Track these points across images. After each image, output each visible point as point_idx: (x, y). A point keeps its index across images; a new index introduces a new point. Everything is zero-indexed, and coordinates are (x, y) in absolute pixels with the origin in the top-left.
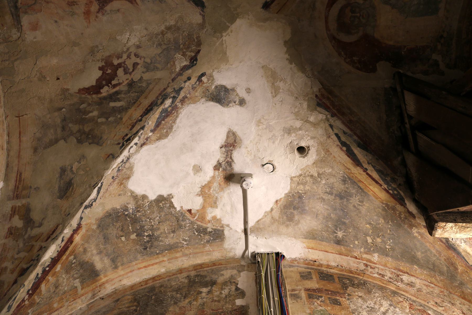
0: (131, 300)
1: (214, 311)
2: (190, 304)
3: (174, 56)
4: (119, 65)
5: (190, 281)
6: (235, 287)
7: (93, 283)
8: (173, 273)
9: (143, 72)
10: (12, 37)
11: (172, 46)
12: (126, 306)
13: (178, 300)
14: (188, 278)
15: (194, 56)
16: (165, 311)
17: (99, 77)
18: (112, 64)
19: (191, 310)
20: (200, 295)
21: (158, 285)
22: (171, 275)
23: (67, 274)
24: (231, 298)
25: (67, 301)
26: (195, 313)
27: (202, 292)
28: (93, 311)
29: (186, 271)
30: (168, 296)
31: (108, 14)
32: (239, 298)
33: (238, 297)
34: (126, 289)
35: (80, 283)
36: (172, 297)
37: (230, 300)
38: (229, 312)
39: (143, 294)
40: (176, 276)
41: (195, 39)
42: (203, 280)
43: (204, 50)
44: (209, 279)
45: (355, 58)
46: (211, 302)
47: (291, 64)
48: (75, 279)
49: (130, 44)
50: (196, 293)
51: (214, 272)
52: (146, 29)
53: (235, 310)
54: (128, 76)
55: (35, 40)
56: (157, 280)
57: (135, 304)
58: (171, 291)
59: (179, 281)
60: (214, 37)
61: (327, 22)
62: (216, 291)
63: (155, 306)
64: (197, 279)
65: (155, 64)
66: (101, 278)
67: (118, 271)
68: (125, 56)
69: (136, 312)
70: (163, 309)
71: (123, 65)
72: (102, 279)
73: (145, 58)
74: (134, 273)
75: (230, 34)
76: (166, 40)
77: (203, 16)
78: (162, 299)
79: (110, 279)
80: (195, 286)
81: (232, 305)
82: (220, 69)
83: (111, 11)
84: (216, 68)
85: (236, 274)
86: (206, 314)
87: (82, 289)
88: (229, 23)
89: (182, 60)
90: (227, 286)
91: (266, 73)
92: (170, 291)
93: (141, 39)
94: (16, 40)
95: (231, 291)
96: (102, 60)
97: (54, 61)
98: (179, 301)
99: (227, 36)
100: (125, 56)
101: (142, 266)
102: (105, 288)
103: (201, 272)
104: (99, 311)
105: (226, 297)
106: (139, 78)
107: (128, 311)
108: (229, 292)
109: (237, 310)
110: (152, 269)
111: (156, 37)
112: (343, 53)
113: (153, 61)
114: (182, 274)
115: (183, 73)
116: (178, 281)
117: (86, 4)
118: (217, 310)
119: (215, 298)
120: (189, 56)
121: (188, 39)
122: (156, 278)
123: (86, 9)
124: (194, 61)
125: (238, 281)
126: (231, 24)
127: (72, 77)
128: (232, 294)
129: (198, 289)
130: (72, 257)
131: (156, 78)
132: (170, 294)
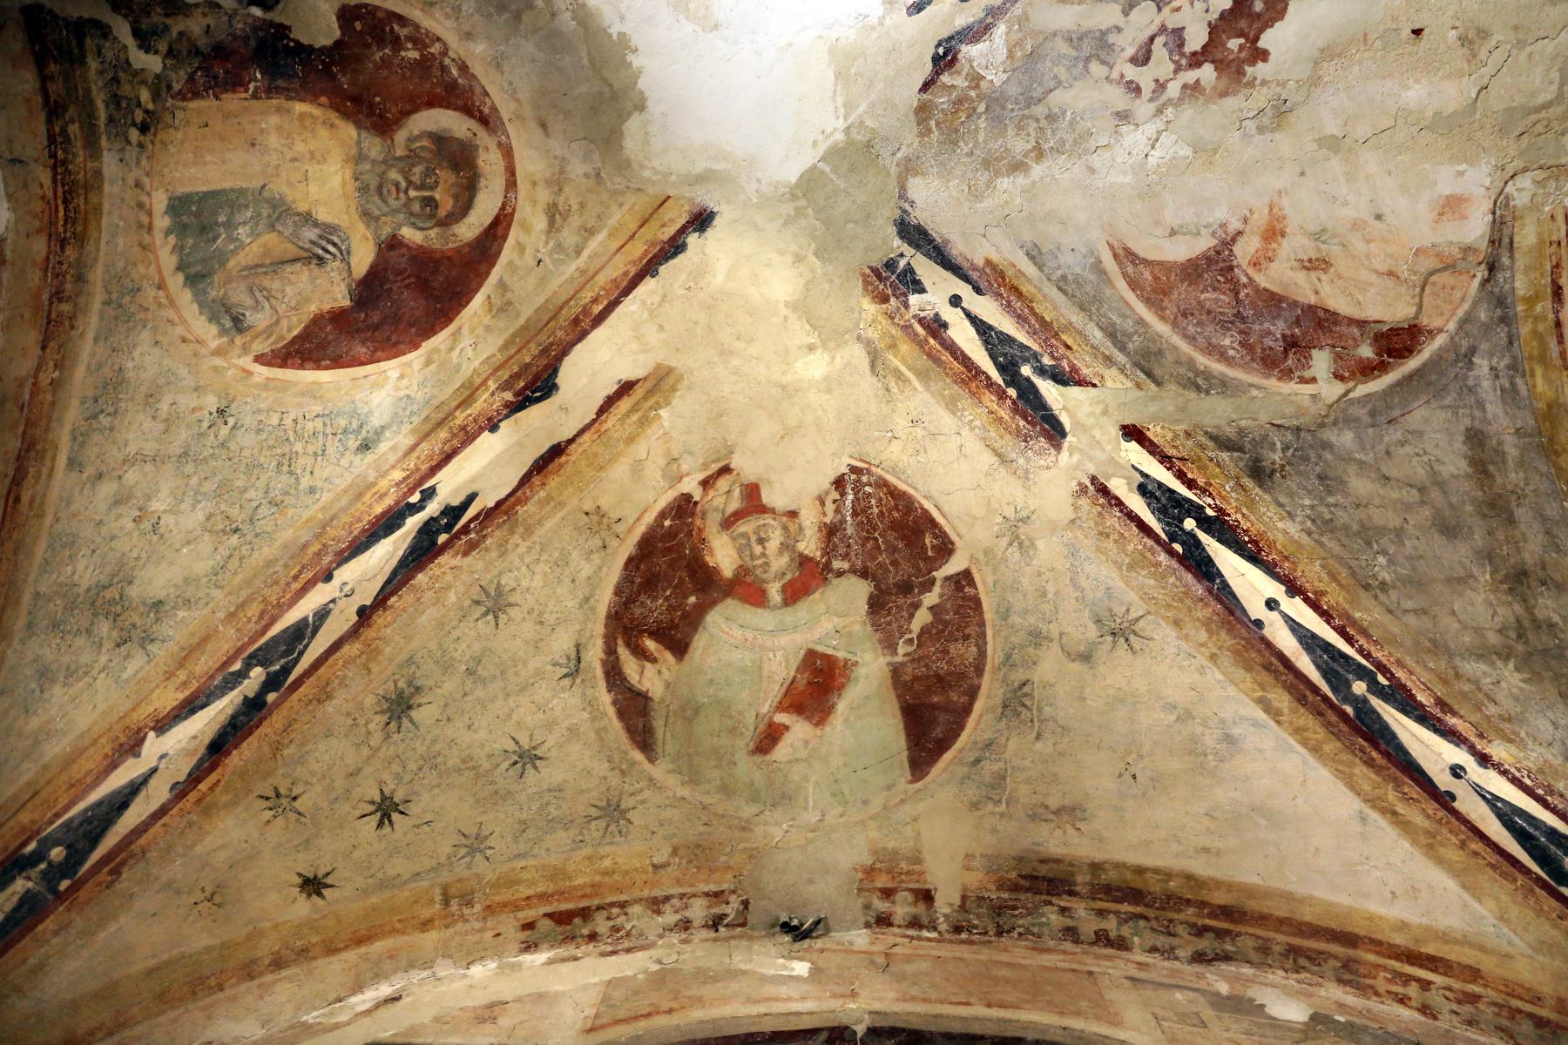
3: (1008, 79)
4: (1196, 60)
9: (1119, 30)
10: (1535, 182)
11: (1012, 110)
15: (943, 71)
17: (1272, 26)
18: (1221, 65)
31: (1205, 227)
41: (934, 129)
43: (909, 92)
45: (414, 55)
47: (622, 35)
49: (1150, 129)
52: (1091, 170)
54: (1173, 21)
55: (1464, 167)
60: (873, 129)
61: (511, 171)
65: (1074, 53)
68: (1173, 89)
71: (1184, 62)
73: (1107, 78)
75: (821, 138)
76: (1031, 130)
77: (903, 196)
82: (859, 25)
83: (1199, 234)
84: (873, 28)
88: (823, 172)
89: (984, 62)
91: (707, 8)
93: (1112, 141)
94: (1525, 170)
96: (1251, 84)
97: (1415, 94)
99: (828, 130)
100: (1173, 89)
106: (1135, 10)
111: (1063, 142)
112: (454, 72)
113: (1081, 65)
115: (982, 15)
117: (1271, 260)
120: (959, 73)
121: (957, 131)
123: (1274, 245)
124: (945, 59)
126: (814, 167)
127: (1366, 35)
131: (1077, 7)
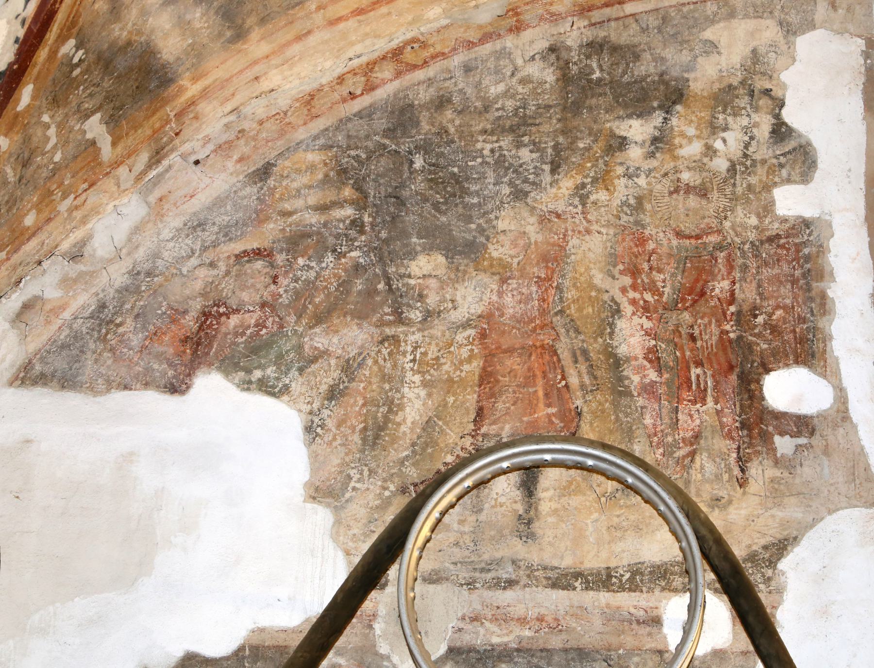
0: (326, 176)
1: (688, 241)
2: (583, 199)
5: (564, 75)
6: (773, 121)
7: (154, 113)
8: (480, 27)
12: (312, 200)
13: (526, 181)
14: (553, 57)
16: (481, 230)
19: (588, 232)
20: (619, 157)
21: (424, 95)
22: (473, 35)
23: (59, 107)
24: (753, 180)
25: (65, 197)
26: (609, 244)
27: (625, 138)
28: (178, 223)
29: (541, 18)
30: (483, 156)
32: (789, 181)
33: (784, 173)
34: (285, 113)
35: (106, 123)
36: (500, 162)
37: (750, 187)
38: (747, 246)
39: (370, 144)
40: (498, 45)
42: (625, 73)
44: (652, 70)
46: (671, 193)
48: (87, 117)
50: (601, 144)
51: (670, 30)
53: (770, 240)
56: (415, 67)
57: (348, 192)
58: (492, 133)
59: (519, 76)
62: (690, 140)
63: (436, 206)
64: (595, 65)
66: (181, 87)
67: (245, 46)
69: (362, 232)
70: (469, 219)
72: (187, 89)
74: (312, 40)
78: (456, 170)
79: (216, 80)
80: (590, 108)
81: (758, 216)
85: (773, 45)
86: (654, 252)
87: (114, 144)
90: (735, 115)
92: (484, 132)
95: (754, 143)
98: (534, 183)
101: (343, 12)
102: (196, 118)
103: (613, 24)
104: (202, 225)
105: (732, 169)
107: (325, 225)
108: (747, 146)
109: (782, 241)
110: (389, 14)
114: (527, 35)
116: (513, 74)
118: (698, 237)
119: (686, 176)
122: (409, 56)
125: (784, 87)
128: (758, 157)
129: (608, 125)
130: (72, 42)
132: (488, 146)
